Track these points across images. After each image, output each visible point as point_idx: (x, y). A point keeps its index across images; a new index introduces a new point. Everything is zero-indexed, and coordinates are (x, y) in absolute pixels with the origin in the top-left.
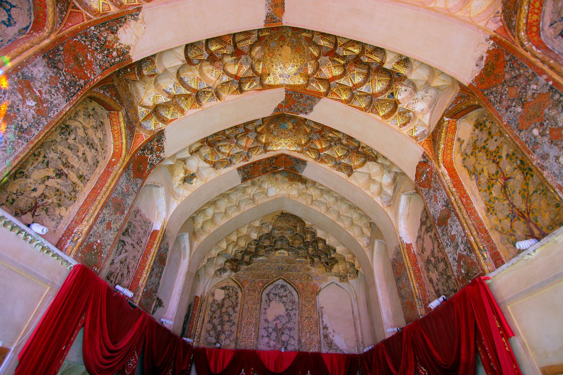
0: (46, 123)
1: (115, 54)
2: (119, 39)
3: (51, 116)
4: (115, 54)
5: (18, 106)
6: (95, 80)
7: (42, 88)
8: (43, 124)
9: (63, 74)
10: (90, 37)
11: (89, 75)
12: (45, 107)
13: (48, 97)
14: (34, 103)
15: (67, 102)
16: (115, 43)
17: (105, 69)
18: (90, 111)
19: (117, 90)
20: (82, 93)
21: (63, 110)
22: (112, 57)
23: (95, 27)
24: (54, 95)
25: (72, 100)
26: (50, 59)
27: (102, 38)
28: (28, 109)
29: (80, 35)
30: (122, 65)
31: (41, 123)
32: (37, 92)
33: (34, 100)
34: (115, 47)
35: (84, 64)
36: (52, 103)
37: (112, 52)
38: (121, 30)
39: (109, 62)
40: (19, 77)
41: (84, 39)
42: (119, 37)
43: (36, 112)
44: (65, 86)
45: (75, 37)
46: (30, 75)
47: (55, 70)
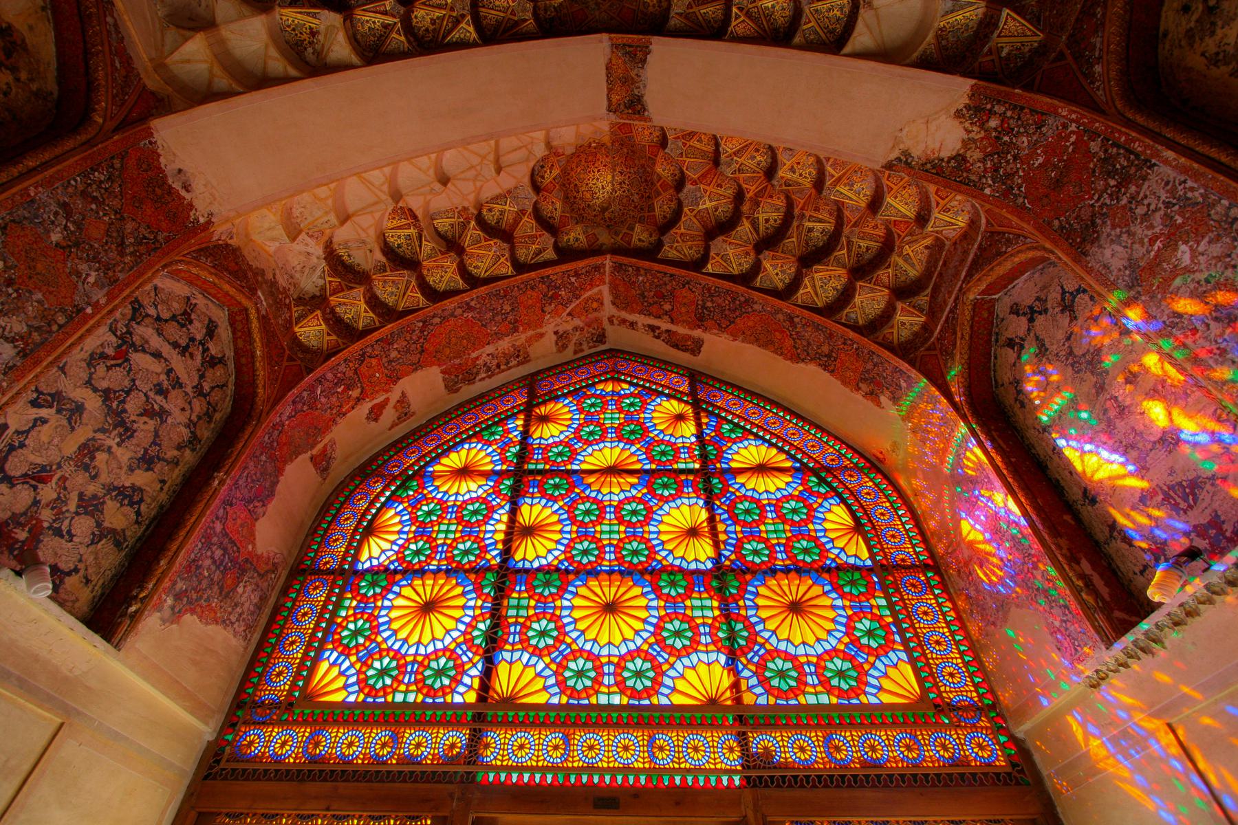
0: (1225, 202)
1: (993, 123)
2: (963, 141)
3: (1202, 195)
4: (993, 123)
5: (1198, 283)
6: (1074, 116)
7: (1142, 239)
8: (1229, 208)
9: (1099, 199)
10: (1004, 184)
11: (1073, 138)
12: (1183, 217)
13: (1157, 219)
14: (1183, 247)
15: (1155, 165)
16: (974, 141)
17: (1037, 113)
18: (1194, 17)
19: (1077, 20)
20: (1120, 132)
21: (1175, 168)
22: (1002, 121)
23: (982, 189)
24: (1149, 205)
25: (1143, 152)
26: (1083, 241)
27: (989, 165)
28: (1200, 258)
29: (1014, 202)
30: (999, 93)
31: (1227, 215)
32: (1156, 248)
33: (1176, 249)
34: (983, 134)
35: (1059, 161)
36: (1168, 205)
37: (995, 129)
38: (945, 154)
39: (1019, 118)
40: (1138, 292)
41: (1015, 191)
42: (959, 145)
43: (1203, 237)
44: (1119, 186)
45: (1023, 207)
46: (1127, 272)
47: (1098, 221)
